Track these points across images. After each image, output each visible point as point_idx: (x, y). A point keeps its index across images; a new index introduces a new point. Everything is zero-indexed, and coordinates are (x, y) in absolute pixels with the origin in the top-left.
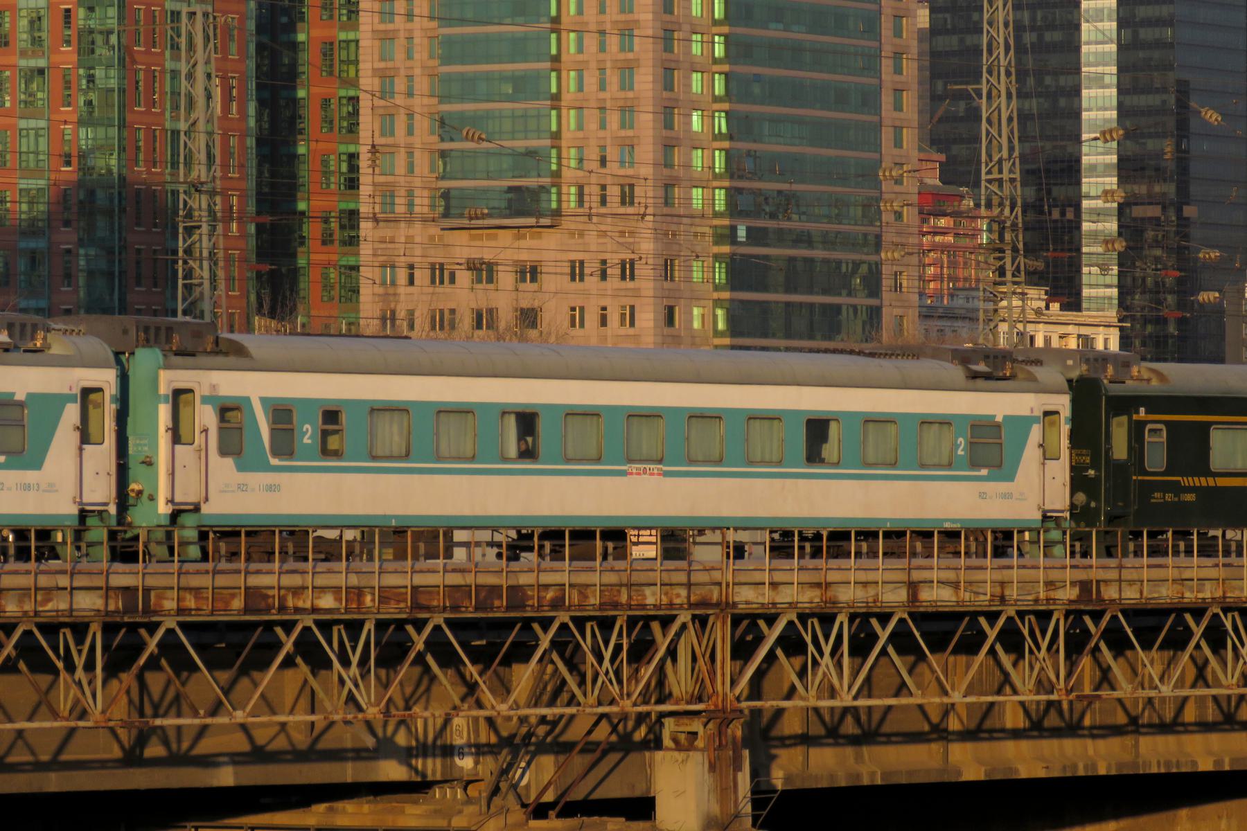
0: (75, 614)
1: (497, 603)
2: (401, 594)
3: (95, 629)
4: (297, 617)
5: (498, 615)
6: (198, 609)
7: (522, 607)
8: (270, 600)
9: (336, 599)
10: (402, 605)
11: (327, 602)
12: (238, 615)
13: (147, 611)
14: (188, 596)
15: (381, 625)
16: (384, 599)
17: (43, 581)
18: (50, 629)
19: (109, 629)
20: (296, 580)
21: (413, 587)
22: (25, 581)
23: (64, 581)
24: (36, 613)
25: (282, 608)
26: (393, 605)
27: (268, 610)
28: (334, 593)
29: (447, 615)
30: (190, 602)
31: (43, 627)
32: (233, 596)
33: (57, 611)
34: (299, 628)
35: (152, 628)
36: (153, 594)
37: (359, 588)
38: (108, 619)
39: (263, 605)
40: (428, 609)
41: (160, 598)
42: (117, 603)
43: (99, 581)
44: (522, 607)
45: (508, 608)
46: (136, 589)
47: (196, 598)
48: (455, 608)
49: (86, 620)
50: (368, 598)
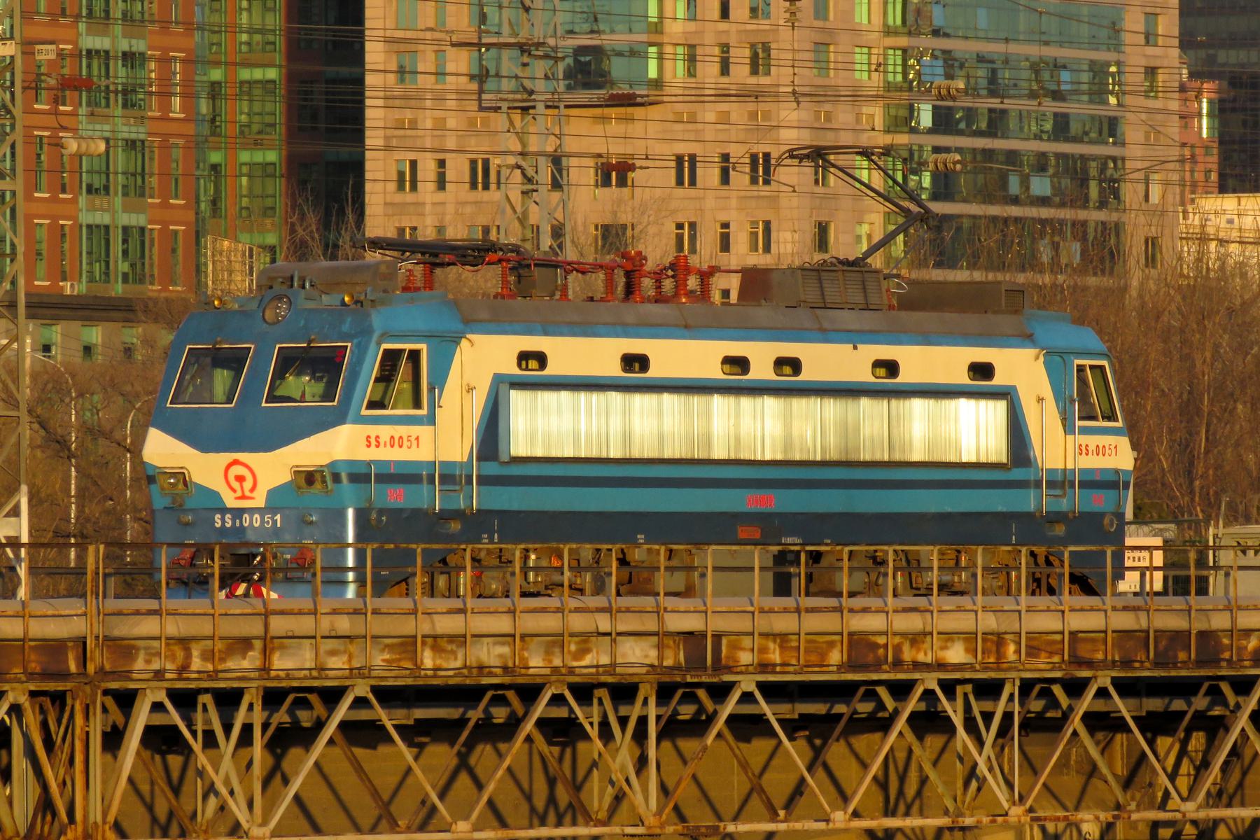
0: (618, 670)
1: (1182, 656)
2: (1054, 642)
3: (647, 690)
4: (916, 676)
5: (1184, 673)
6: (783, 665)
7: (1215, 662)
8: (881, 651)
9: (967, 650)
10: (1056, 659)
11: (956, 654)
12: (838, 672)
13: (718, 666)
14: (771, 645)
15: (1026, 687)
16: (1033, 651)
17: (578, 623)
18: (584, 692)
19: (665, 693)
20: (913, 623)
21: (1071, 633)
22: (550, 623)
23: (604, 623)
24: (571, 671)
25: (898, 664)
26: (1043, 658)
27: (877, 667)
28: (966, 640)
29: (1115, 674)
30: (775, 656)
31: (574, 688)
32: (831, 645)
33: (597, 666)
34: (919, 691)
35: (720, 692)
36: (724, 641)
37: (999, 635)
38: (666, 679)
39: (870, 658)
40: (1090, 664)
41: (735, 647)
42: (676, 655)
43: (651, 625)
44: (1215, 662)
45: (1200, 663)
46: (703, 635)
47: (781, 647)
48: (1126, 663)
49: (636, 679)
50: (1012, 648)
